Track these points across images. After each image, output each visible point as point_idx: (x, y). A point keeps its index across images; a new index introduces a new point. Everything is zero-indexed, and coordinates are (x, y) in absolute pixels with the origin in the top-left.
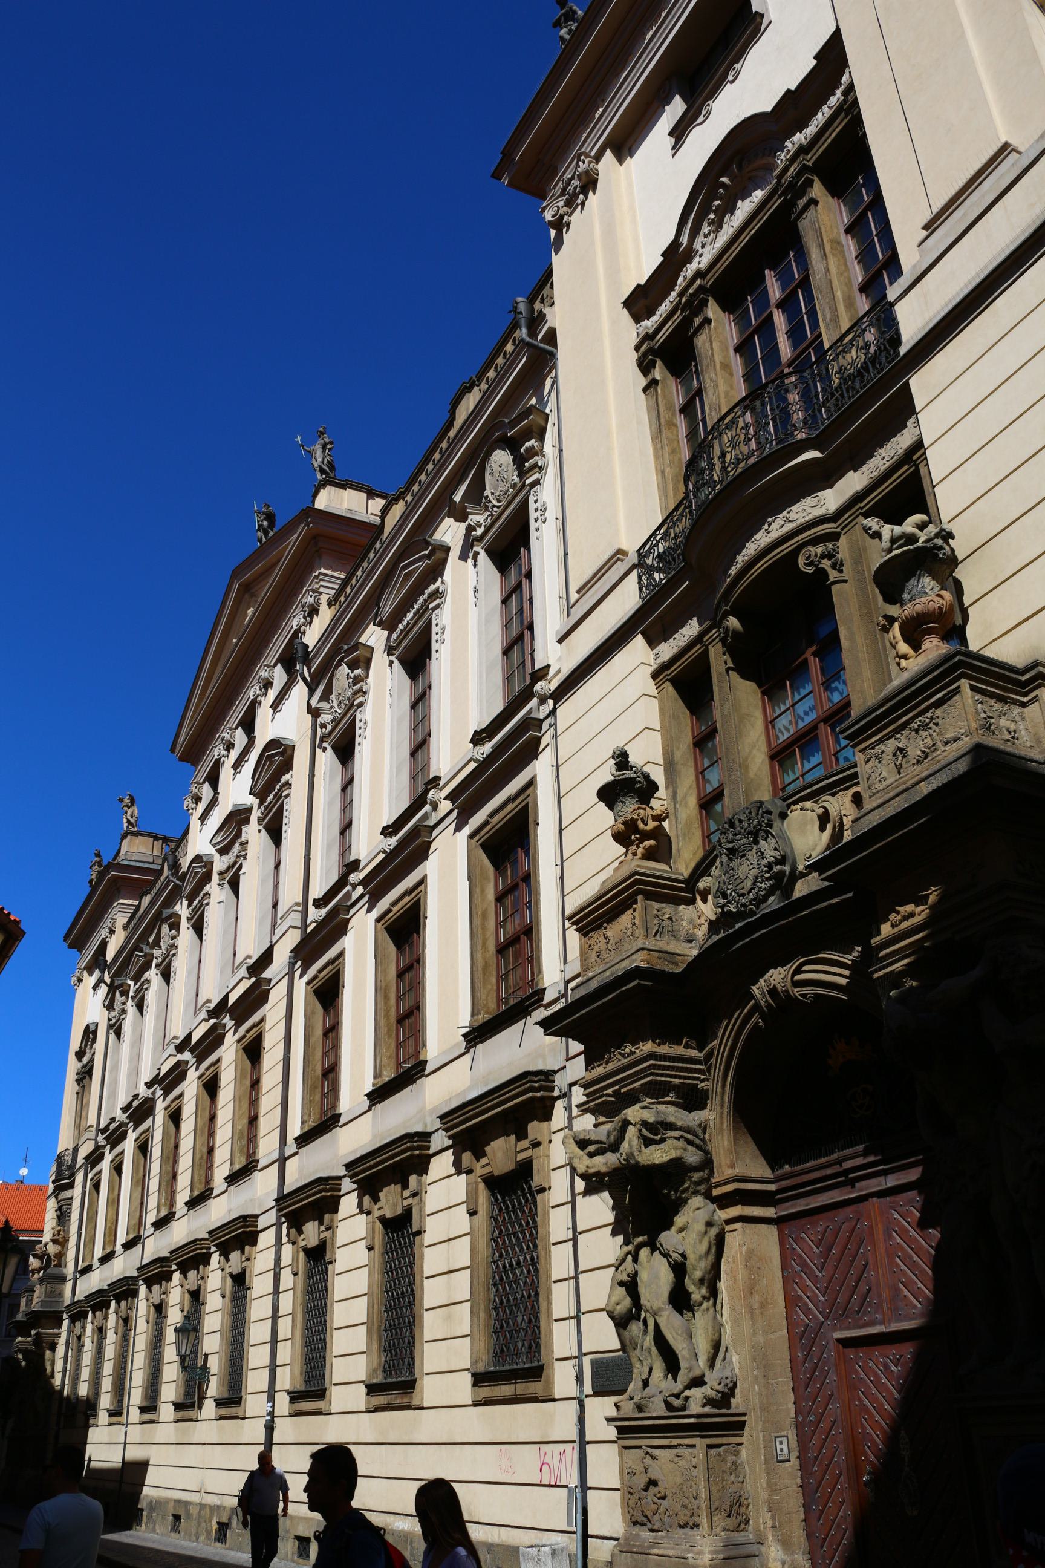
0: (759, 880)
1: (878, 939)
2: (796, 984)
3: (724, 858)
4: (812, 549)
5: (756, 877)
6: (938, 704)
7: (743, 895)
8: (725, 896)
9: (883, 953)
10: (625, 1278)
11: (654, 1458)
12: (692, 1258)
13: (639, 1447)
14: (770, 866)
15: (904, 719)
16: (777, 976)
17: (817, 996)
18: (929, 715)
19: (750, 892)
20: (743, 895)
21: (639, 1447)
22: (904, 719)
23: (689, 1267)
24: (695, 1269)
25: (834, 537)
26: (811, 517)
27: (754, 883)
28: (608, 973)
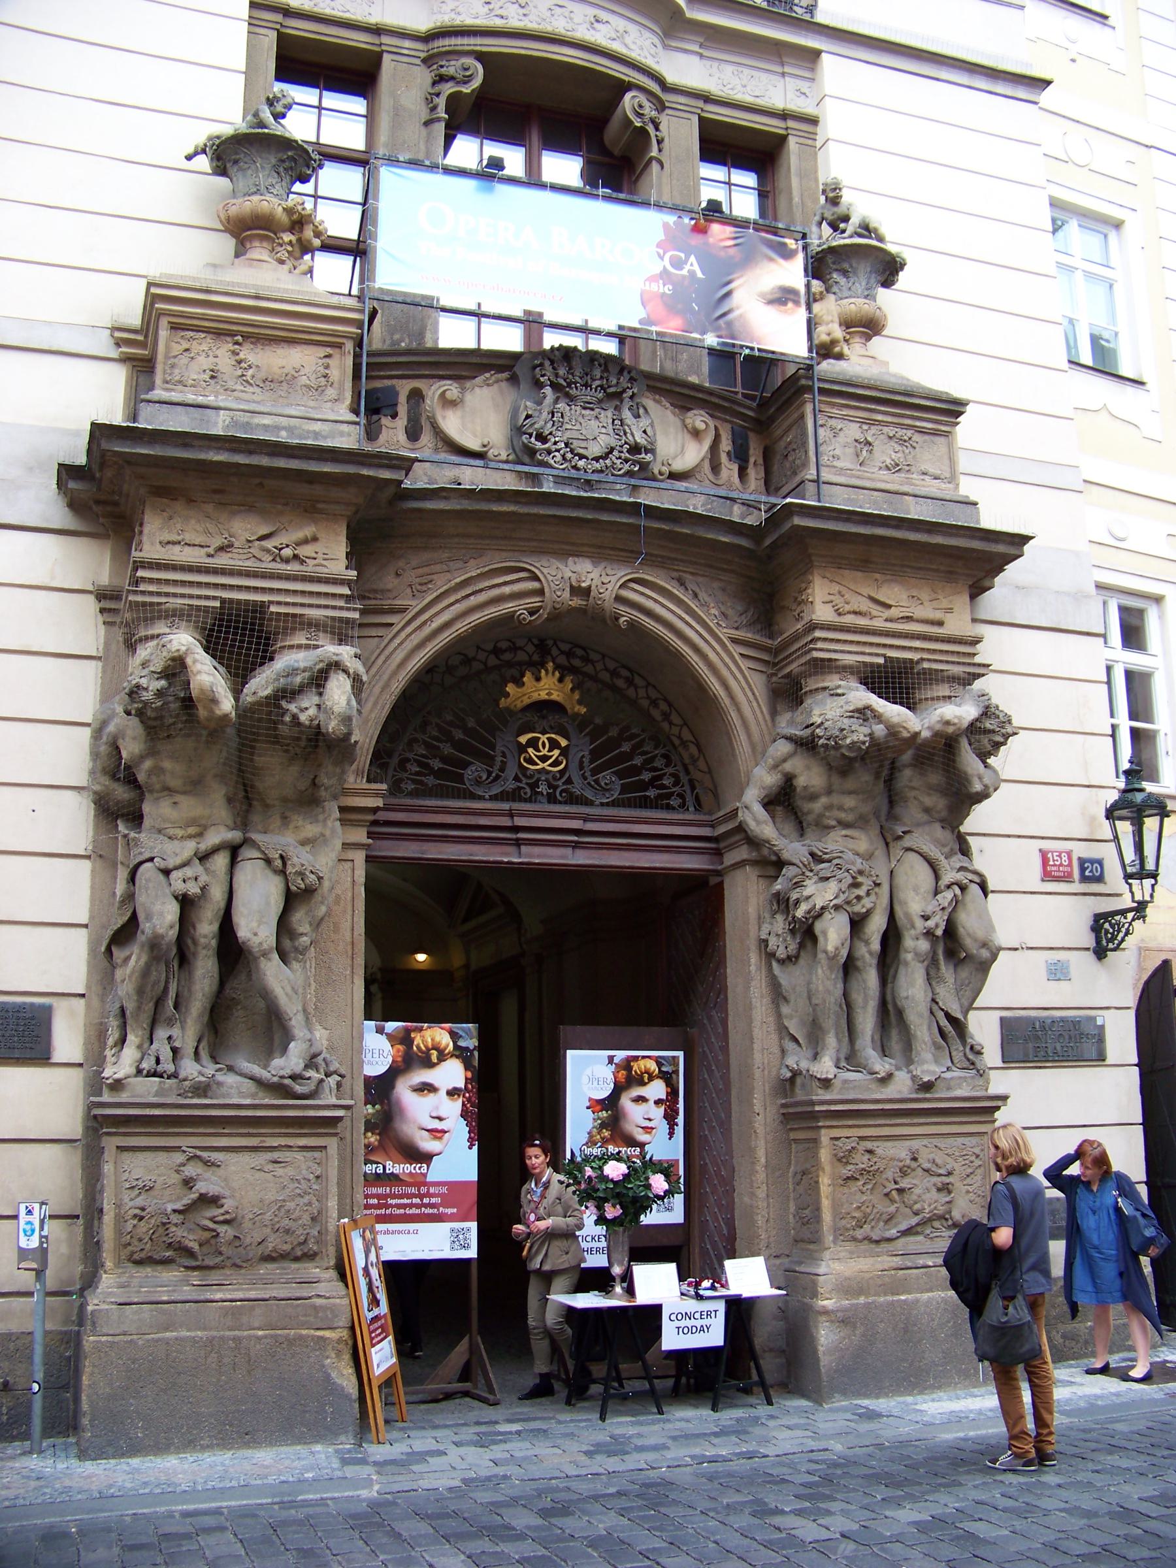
0: (616, 453)
2: (619, 599)
3: (548, 390)
4: (642, 98)
5: (612, 450)
6: (922, 431)
7: (581, 457)
8: (542, 438)
9: (818, 634)
10: (193, 889)
11: (208, 1164)
13: (177, 1149)
14: (635, 449)
15: (880, 417)
16: (602, 579)
17: (632, 624)
18: (909, 433)
19: (597, 459)
20: (581, 457)
21: (177, 1149)
22: (880, 417)
23: (317, 897)
24: (322, 903)
25: (661, 106)
26: (644, 61)
27: (605, 456)
28: (267, 420)
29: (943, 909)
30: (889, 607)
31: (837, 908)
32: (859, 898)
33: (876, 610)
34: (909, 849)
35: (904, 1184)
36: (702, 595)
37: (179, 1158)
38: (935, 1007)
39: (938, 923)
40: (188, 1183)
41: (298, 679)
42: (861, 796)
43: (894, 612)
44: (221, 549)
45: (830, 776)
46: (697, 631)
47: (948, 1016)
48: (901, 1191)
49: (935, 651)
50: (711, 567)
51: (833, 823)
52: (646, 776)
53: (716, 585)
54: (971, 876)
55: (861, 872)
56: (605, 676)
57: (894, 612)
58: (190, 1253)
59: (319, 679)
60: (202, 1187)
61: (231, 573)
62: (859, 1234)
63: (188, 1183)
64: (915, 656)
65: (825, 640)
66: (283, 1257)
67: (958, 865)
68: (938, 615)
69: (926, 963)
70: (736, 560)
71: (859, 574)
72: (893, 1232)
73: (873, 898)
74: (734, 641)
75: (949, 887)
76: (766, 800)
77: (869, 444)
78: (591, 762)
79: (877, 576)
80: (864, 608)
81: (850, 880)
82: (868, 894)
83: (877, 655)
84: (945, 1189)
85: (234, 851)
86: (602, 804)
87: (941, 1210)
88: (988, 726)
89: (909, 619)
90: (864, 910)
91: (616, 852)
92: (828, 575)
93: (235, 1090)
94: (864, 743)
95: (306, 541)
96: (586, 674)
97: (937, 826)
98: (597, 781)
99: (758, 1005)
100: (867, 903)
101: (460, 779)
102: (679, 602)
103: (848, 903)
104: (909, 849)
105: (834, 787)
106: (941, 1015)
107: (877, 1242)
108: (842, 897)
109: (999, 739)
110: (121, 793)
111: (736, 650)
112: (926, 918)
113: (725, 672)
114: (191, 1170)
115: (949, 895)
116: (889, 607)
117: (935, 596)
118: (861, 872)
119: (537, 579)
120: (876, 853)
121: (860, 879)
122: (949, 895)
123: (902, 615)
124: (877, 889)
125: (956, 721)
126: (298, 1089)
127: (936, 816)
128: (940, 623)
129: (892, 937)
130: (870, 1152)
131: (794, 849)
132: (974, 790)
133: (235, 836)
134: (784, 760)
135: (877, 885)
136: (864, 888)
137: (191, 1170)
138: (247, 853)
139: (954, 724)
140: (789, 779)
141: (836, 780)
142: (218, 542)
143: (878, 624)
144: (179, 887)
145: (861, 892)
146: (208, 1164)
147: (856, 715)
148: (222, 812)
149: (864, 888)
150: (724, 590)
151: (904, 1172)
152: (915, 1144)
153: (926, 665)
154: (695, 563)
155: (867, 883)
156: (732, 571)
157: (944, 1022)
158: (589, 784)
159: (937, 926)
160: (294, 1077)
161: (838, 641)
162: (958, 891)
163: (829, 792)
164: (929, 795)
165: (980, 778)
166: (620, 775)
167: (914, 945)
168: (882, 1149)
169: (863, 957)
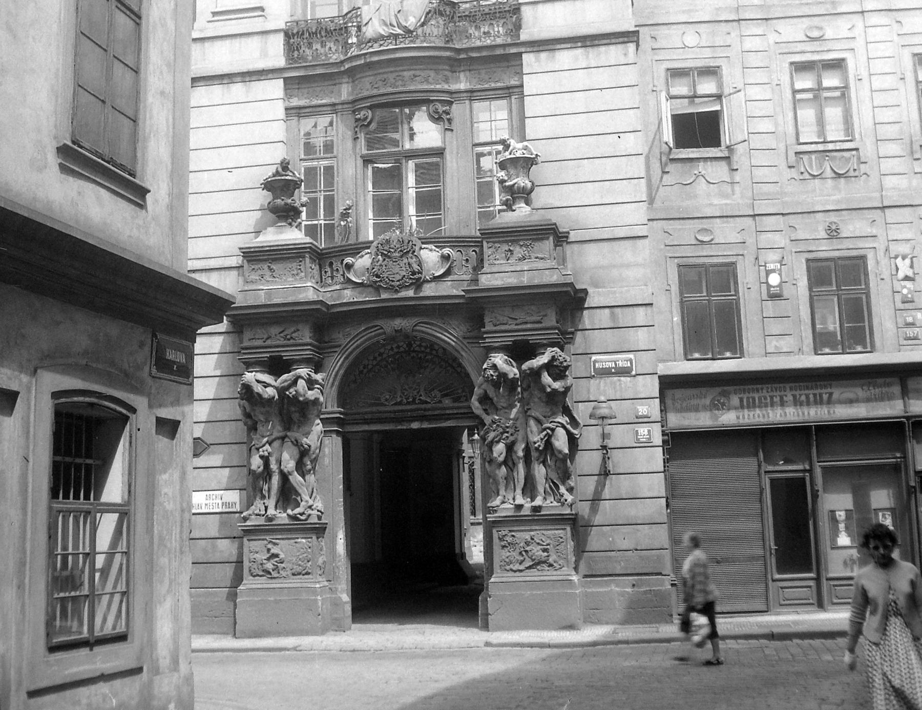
8: (378, 276)
10: (266, 454)
11: (275, 544)
12: (313, 449)
14: (414, 273)
35: (528, 549)
37: (265, 542)
40: (269, 550)
41: (286, 384)
44: (268, 339)
48: (526, 551)
57: (518, 322)
58: (269, 573)
59: (295, 382)
60: (272, 551)
61: (270, 347)
62: (508, 568)
63: (269, 550)
66: (299, 574)
72: (521, 567)
73: (515, 436)
77: (510, 250)
84: (545, 550)
85: (283, 438)
87: (543, 559)
89: (526, 323)
93: (282, 517)
95: (295, 332)
100: (512, 438)
101: (379, 399)
107: (515, 571)
110: (250, 423)
111: (465, 342)
114: (270, 546)
115: (545, 433)
119: (382, 328)
122: (545, 433)
126: (303, 518)
129: (527, 450)
130: (513, 536)
131: (487, 419)
133: (281, 434)
137: (270, 546)
138: (286, 440)
140: (486, 392)
142: (265, 337)
144: (261, 453)
146: (275, 544)
148: (279, 428)
151: (527, 543)
152: (532, 533)
155: (511, 431)
160: (301, 514)
167: (534, 454)
168: (517, 535)
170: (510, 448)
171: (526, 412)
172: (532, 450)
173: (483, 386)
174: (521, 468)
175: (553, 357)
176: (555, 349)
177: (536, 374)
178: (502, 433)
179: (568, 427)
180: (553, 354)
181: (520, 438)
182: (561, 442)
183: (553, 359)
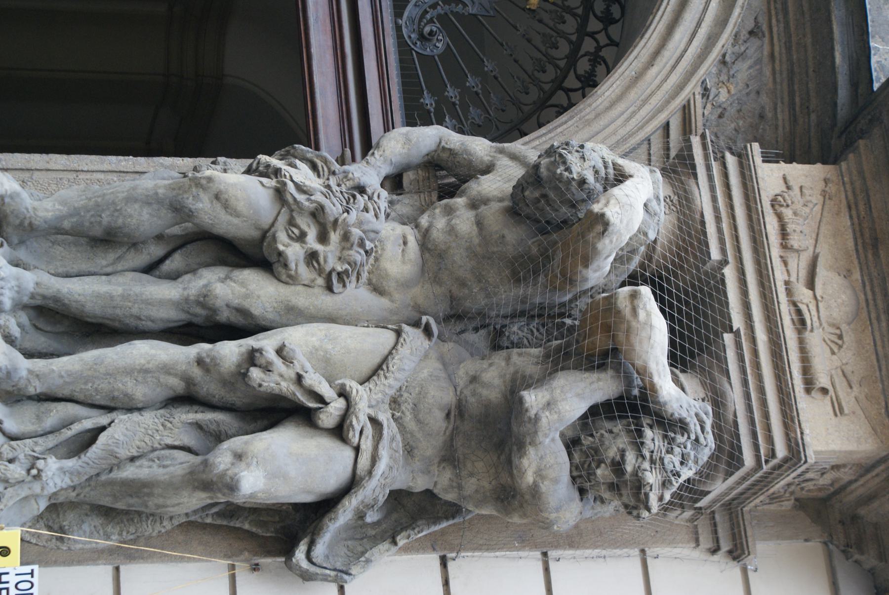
1: (758, 159)
9: (731, 161)
29: (299, 378)
30: (811, 285)
31: (280, 192)
32: (302, 237)
33: (799, 266)
34: (399, 333)
36: (743, 70)
38: (113, 415)
39: (275, 381)
42: (476, 241)
43: (803, 294)
45: (501, 200)
46: (685, 51)
47: (103, 429)
49: (757, 366)
50: (791, 73)
51: (424, 221)
52: (451, 92)
53: (764, 99)
54: (367, 445)
55: (346, 237)
56: (588, 45)
57: (803, 294)
64: (737, 322)
65: (725, 175)
67: (384, 417)
68: (823, 380)
69: (197, 372)
70: (813, 117)
71: (851, 244)
73: (305, 272)
74: (686, 110)
75: (343, 393)
76: (445, 155)
78: (456, 14)
79: (857, 275)
80: (795, 241)
81: (334, 209)
82: (312, 257)
83: (723, 251)
86: (398, 28)
88: (648, 433)
89: (801, 323)
90: (281, 248)
91: (330, 43)
92: (832, 188)
94: (568, 169)
96: (585, 20)
97: (448, 397)
98: (431, 21)
99: (105, 167)
100: (294, 252)
102: (722, 22)
103: (292, 223)
104: (399, 333)
105: (483, 208)
106: (103, 420)
108: (301, 198)
109: (631, 460)
111: (672, 114)
112: (280, 352)
113: (633, 95)
116: (811, 285)
117: (854, 379)
118: (346, 237)
120: (384, 302)
121: (334, 237)
123: (803, 308)
124: (320, 281)
125: (642, 315)
127: (467, 392)
128: (808, 391)
132: (525, 394)
134: (514, 157)
135: (329, 288)
136: (318, 247)
139: (634, 311)
141: (495, 206)
143: (780, 275)
145: (312, 241)
147: (611, 171)
149: (318, 247)
150: (762, 117)
153: (728, 338)
154: (789, 49)
155: (330, 255)
156: (794, 119)
157: (88, 424)
158: (426, 12)
159: (267, 368)
161: (729, 196)
162: (337, 406)
163: (474, 205)
164: (502, 376)
165: (549, 405)
166: (447, 54)
167: (229, 351)
169: (200, 277)
170: (251, 253)
171: (416, 324)
172: (250, 342)
173: (504, 162)
174: (162, 296)
175: (682, 426)
176: (709, 441)
177: (597, 344)
178: (317, 214)
179: (345, 514)
180: (694, 426)
181: (299, 297)
182: (276, 466)
183: (671, 426)
